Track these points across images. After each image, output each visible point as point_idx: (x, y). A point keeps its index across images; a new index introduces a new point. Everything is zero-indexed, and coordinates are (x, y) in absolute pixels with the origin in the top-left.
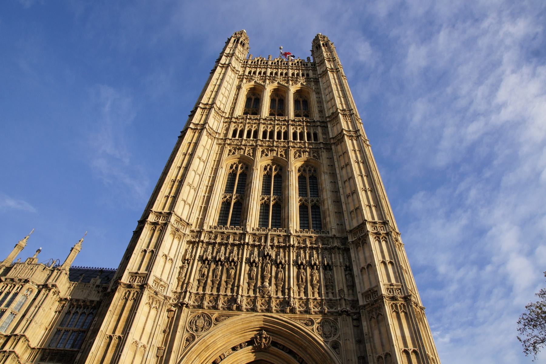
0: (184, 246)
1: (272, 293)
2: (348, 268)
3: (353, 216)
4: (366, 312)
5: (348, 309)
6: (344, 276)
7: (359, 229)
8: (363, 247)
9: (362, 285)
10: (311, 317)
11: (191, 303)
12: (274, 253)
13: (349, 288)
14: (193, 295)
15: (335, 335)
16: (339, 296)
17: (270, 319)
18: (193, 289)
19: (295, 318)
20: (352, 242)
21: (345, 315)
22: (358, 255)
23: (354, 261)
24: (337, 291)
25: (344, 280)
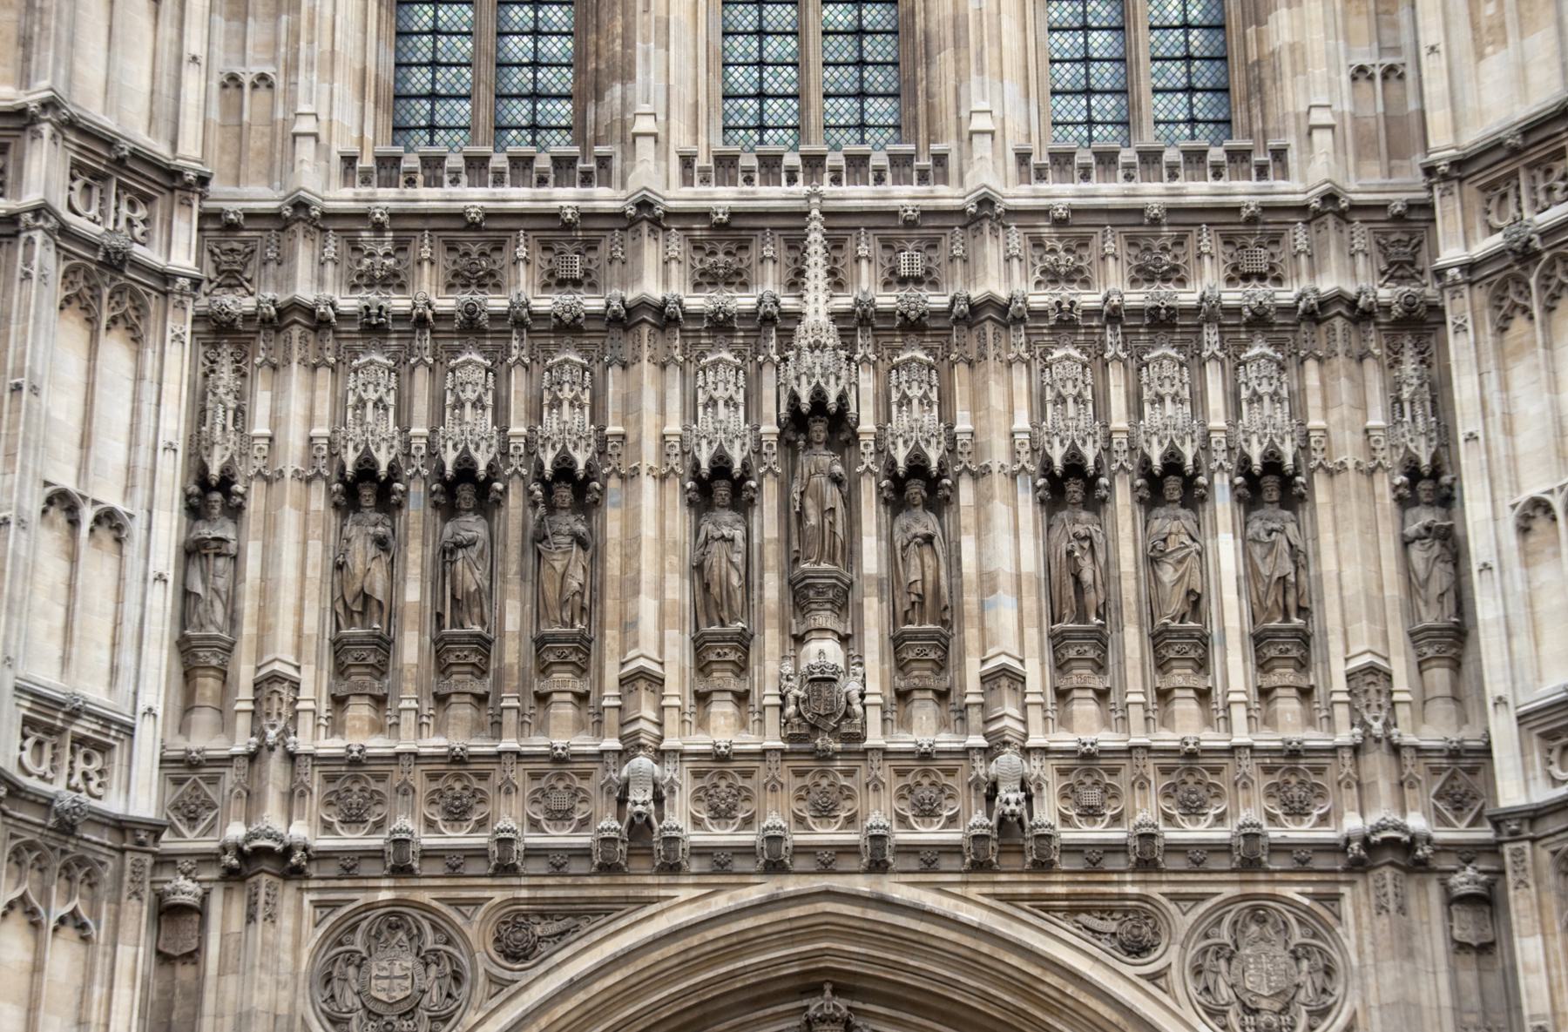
1: (874, 716)
2: (1424, 486)
4: (1545, 855)
5: (1417, 822)
6: (1389, 547)
7: (1535, 154)
8: (1546, 327)
9: (1522, 644)
10: (1154, 891)
11: (300, 831)
12: (867, 382)
13: (1430, 652)
14: (315, 780)
16: (1357, 719)
17: (872, 914)
18: (306, 722)
19: (1044, 905)
20: (1470, 267)
21: (1389, 873)
22: (1505, 386)
23: (1472, 437)
24: (1340, 683)
25: (1393, 589)
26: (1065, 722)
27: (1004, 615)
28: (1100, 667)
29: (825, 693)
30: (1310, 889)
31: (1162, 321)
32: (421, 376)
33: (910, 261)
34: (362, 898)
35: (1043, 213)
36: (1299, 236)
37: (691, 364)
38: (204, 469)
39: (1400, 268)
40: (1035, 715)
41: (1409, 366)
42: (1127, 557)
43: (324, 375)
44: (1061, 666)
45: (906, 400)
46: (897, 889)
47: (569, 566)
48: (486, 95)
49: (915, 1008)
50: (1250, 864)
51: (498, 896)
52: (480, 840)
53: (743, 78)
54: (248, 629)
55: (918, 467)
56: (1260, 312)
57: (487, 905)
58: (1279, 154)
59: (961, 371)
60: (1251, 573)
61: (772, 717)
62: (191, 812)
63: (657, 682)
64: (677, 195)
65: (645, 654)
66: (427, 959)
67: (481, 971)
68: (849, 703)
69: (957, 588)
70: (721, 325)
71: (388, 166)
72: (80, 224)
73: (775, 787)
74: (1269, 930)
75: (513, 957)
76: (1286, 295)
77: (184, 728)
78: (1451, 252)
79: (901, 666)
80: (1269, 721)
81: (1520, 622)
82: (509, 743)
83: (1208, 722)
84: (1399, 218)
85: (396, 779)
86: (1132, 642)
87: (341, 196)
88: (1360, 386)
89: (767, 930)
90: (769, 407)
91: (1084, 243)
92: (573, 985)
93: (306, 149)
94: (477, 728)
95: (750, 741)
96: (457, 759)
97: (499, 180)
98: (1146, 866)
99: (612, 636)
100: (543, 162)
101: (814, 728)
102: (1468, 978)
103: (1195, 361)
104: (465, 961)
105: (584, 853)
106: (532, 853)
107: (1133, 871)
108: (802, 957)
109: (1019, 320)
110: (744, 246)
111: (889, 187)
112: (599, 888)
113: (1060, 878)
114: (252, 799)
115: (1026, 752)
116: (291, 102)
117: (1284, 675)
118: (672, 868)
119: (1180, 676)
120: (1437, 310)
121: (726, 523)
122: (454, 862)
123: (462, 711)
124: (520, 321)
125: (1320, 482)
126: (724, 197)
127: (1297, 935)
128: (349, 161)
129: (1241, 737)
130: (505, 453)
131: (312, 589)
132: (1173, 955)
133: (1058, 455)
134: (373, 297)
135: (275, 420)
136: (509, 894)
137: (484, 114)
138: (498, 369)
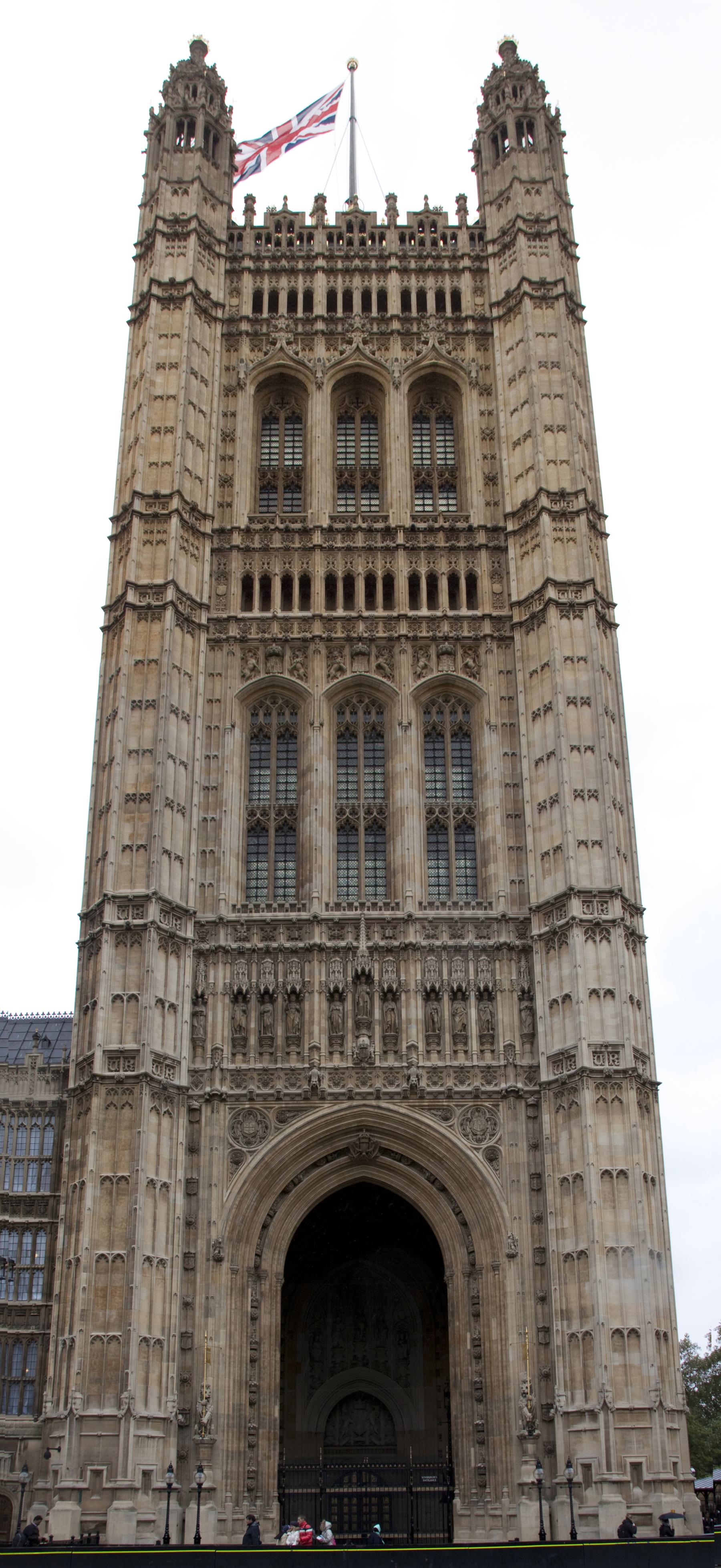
0: (189, 963)
1: (377, 1058)
3: (547, 865)
5: (520, 1085)
6: (516, 1012)
11: (224, 1089)
12: (377, 966)
14: (228, 1076)
15: (493, 1135)
16: (506, 1058)
18: (225, 1060)
19: (422, 1108)
20: (540, 936)
22: (548, 968)
24: (502, 1048)
25: (517, 1023)
26: (429, 1059)
27: (413, 1030)
28: (438, 1044)
31: (458, 949)
32: (254, 965)
33: (389, 932)
35: (426, 919)
36: (495, 926)
37: (328, 961)
38: (196, 992)
39: (522, 935)
40: (421, 1057)
41: (523, 963)
42: (447, 1014)
43: (228, 966)
44: (428, 1044)
45: (387, 971)
46: (384, 1104)
47: (295, 1017)
48: (271, 887)
49: (387, 1135)
50: (477, 1097)
52: (272, 1091)
53: (342, 881)
54: (209, 1035)
55: (390, 990)
58: (490, 904)
59: (402, 963)
60: (479, 1019)
61: (350, 1058)
62: (196, 1084)
63: (319, 1049)
64: (324, 914)
65: (315, 1042)
66: (259, 1123)
69: (400, 1023)
70: (336, 950)
71: (245, 907)
72: (163, 926)
73: (351, 1077)
76: (491, 943)
77: (193, 1062)
78: (535, 932)
79: (385, 1044)
80: (483, 1059)
81: (549, 1032)
82: (279, 1066)
83: (467, 1059)
84: (522, 922)
85: (249, 1075)
86: (447, 1037)
87: (232, 916)
88: (510, 968)
90: (349, 973)
91: (437, 927)
93: (222, 903)
94: (270, 1062)
95: (344, 1065)
96: (265, 1070)
97: (275, 911)
99: (306, 1037)
100: (287, 906)
102: (530, 1126)
103: (466, 961)
105: (299, 1095)
106: (286, 1095)
109: (418, 949)
110: (343, 928)
111: (383, 912)
112: (303, 1104)
114: (212, 1081)
115: (418, 1067)
116: (218, 890)
117: (487, 1047)
119: (460, 1047)
120: (531, 947)
121: (338, 1005)
122: (265, 1097)
123: (266, 1057)
124: (281, 950)
125: (499, 994)
126: (337, 915)
127: (488, 1115)
128: (234, 906)
129: (475, 1063)
130: (277, 986)
131: (226, 1025)
132: (455, 1121)
133: (428, 986)
134: (241, 944)
135: (215, 978)
137: (271, 893)
138: (275, 963)
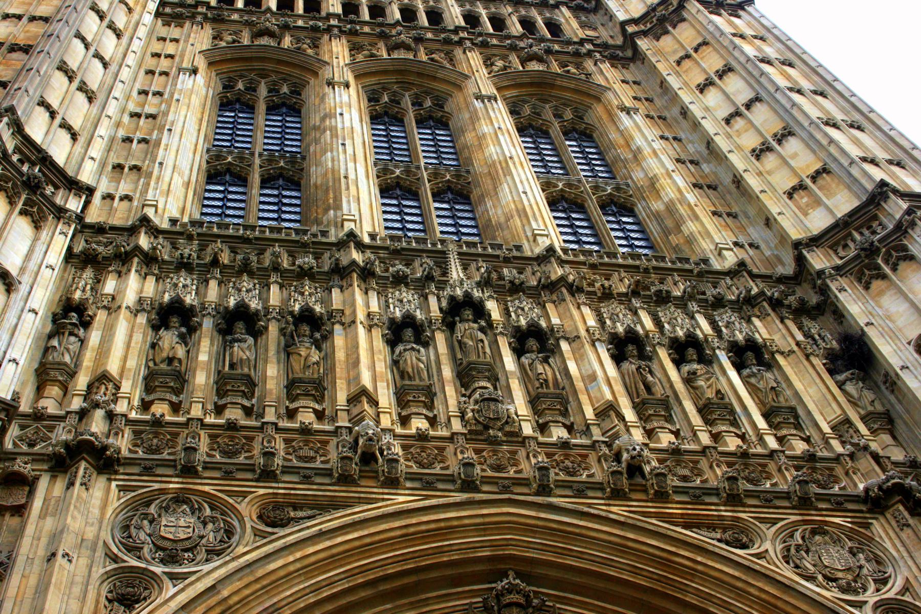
29: (493, 407)
30: (849, 520)
34: (157, 486)
51: (262, 491)
56: (720, 297)
57: (250, 497)
67: (248, 526)
68: (509, 417)
74: (827, 538)
75: (273, 525)
89: (467, 521)
92: (321, 535)
98: (734, 500)
101: (487, 427)
104: (236, 523)
107: (725, 505)
108: (493, 545)
113: (674, 506)
118: (392, 483)
136: (271, 491)
